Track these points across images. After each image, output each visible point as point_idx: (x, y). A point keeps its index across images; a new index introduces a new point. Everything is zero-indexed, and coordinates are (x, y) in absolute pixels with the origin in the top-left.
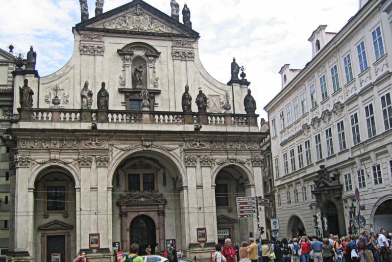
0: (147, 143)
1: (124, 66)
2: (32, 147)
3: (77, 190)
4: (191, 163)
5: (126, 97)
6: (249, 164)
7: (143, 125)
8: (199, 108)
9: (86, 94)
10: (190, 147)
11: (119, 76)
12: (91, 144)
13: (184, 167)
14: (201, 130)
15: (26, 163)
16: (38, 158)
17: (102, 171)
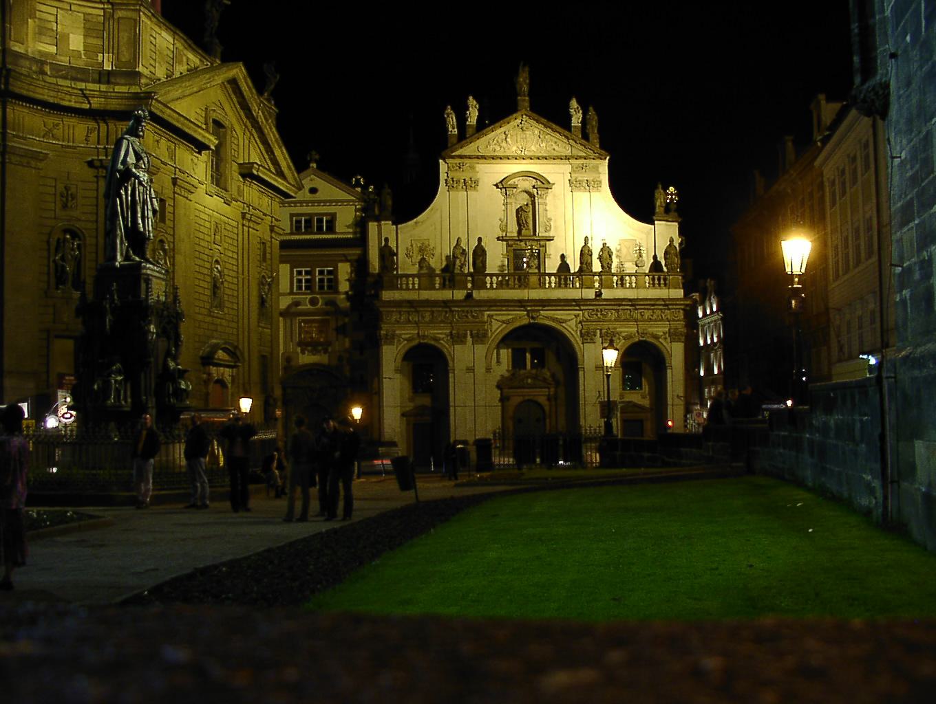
0: (534, 315)
1: (506, 204)
2: (398, 322)
3: (450, 371)
4: (589, 338)
5: (508, 245)
6: (665, 338)
7: (530, 291)
8: (602, 266)
9: (459, 251)
10: (589, 318)
11: (498, 218)
12: (467, 316)
13: (580, 342)
14: (603, 297)
15: (391, 339)
16: (404, 334)
17: (481, 350)
